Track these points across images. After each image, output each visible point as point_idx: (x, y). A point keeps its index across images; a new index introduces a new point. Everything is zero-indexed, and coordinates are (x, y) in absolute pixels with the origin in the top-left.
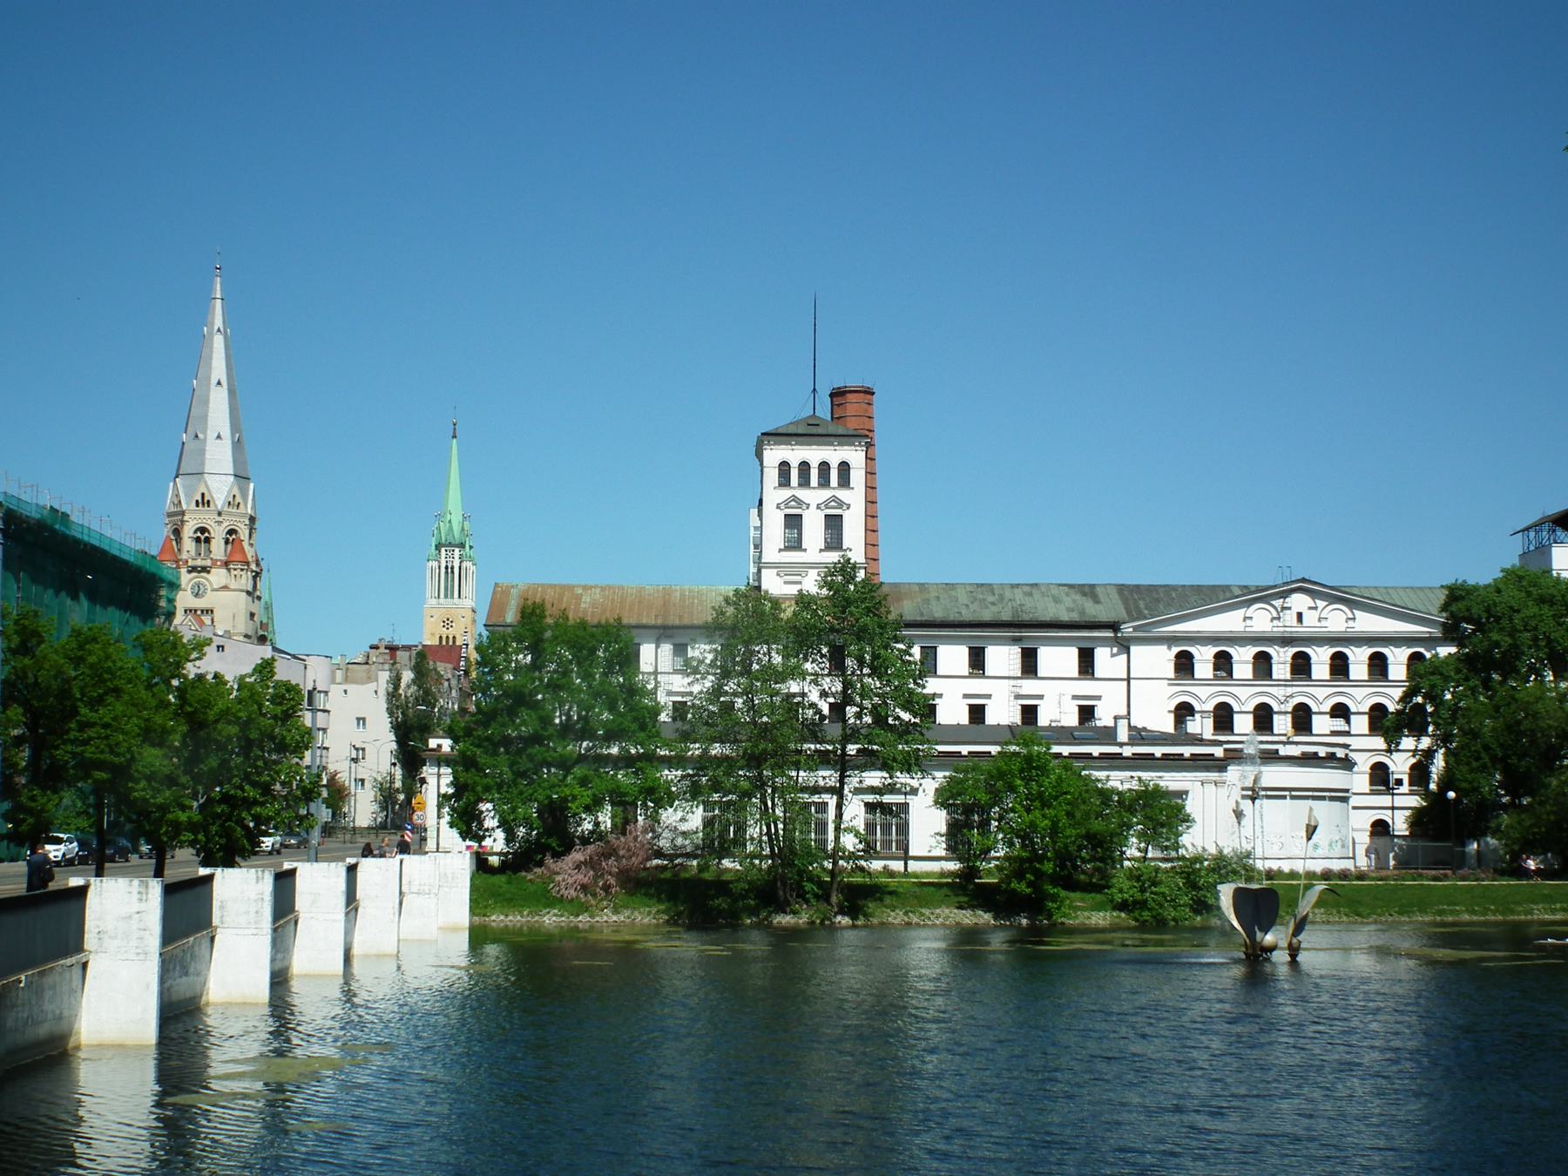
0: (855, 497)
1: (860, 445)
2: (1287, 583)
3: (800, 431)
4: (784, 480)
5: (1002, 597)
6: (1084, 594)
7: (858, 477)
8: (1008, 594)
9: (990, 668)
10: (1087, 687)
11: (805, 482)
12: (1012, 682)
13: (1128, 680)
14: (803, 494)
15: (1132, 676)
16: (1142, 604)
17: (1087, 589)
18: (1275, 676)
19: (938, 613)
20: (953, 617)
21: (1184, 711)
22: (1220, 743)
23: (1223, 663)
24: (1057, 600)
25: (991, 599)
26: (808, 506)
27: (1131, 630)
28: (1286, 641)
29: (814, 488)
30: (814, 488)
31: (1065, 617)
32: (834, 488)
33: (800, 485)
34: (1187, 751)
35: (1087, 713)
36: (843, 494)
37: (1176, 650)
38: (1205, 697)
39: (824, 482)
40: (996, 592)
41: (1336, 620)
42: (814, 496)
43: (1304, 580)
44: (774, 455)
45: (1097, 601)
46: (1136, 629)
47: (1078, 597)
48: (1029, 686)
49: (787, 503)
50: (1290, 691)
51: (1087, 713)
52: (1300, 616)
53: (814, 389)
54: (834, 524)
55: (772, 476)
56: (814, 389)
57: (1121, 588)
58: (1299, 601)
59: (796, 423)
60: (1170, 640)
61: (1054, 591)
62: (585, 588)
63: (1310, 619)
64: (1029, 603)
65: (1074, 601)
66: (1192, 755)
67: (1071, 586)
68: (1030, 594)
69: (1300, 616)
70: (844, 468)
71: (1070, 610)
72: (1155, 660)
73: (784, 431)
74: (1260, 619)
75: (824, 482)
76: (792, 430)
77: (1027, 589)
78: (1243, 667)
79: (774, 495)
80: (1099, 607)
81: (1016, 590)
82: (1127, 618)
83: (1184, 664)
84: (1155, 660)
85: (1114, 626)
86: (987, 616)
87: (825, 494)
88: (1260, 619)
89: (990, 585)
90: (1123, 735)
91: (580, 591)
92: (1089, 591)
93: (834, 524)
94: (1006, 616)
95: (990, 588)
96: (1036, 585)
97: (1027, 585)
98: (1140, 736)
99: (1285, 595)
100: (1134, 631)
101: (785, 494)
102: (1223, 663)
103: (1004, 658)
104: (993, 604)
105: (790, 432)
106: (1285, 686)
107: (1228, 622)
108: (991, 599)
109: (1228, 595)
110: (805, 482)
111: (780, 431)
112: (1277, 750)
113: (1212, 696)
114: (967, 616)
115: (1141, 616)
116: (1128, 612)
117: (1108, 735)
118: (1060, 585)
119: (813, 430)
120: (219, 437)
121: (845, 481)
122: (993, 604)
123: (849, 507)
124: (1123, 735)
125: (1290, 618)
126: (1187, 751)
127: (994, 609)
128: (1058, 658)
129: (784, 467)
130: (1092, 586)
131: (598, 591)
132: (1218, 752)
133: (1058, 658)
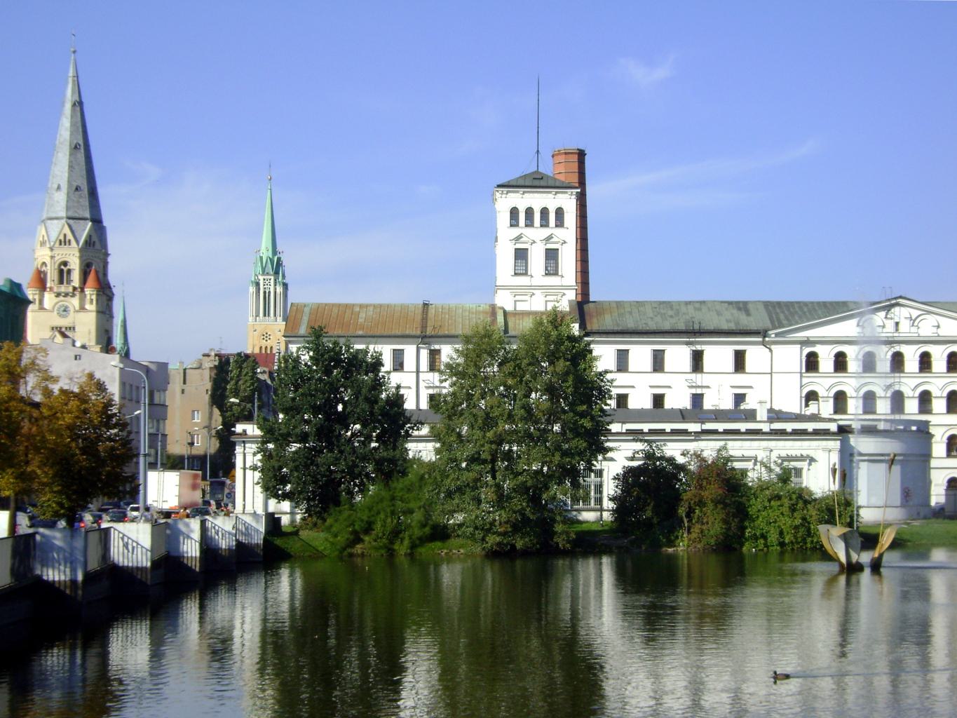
0: (569, 233)
1: (572, 194)
2: (889, 300)
3: (527, 184)
5: (677, 313)
6: (739, 309)
8: (683, 309)
9: (668, 366)
10: (740, 379)
11: (529, 222)
13: (771, 373)
14: (529, 232)
15: (773, 371)
16: (782, 316)
17: (741, 305)
19: (630, 324)
20: (641, 327)
21: (812, 396)
22: (835, 420)
24: (719, 314)
25: (670, 313)
26: (534, 242)
27: (773, 336)
28: (890, 342)
31: (725, 326)
33: (526, 226)
34: (810, 426)
35: (739, 398)
36: (560, 233)
37: (807, 350)
39: (545, 223)
40: (674, 307)
41: (927, 327)
42: (537, 233)
44: (506, 202)
45: (748, 313)
46: (777, 335)
47: (735, 311)
48: (698, 378)
49: (518, 239)
50: (890, 381)
51: (739, 398)
52: (897, 324)
55: (504, 218)
57: (768, 305)
61: (718, 307)
62: (361, 306)
63: (905, 327)
64: (698, 316)
65: (732, 314)
67: (730, 303)
68: (700, 309)
70: (560, 213)
71: (728, 321)
72: (789, 357)
73: (515, 184)
75: (545, 223)
76: (521, 182)
77: (697, 305)
79: (505, 233)
80: (751, 319)
81: (690, 307)
82: (771, 327)
83: (812, 363)
84: (789, 357)
86: (667, 326)
87: (545, 232)
89: (669, 302)
90: (762, 414)
91: (357, 309)
92: (743, 307)
93: (552, 255)
94: (682, 327)
95: (668, 304)
96: (704, 302)
97: (697, 302)
98: (775, 415)
99: (889, 308)
101: (515, 232)
102: (840, 363)
103: (679, 356)
104: (671, 317)
105: (518, 184)
106: (886, 377)
107: (847, 328)
108: (670, 313)
109: (845, 309)
110: (529, 222)
111: (511, 184)
112: (876, 425)
114: (652, 326)
115: (781, 326)
116: (772, 322)
117: (751, 415)
118: (722, 302)
119: (537, 183)
121: (560, 222)
122: (671, 317)
124: (762, 414)
125: (890, 326)
126: (810, 426)
127: (673, 321)
129: (514, 213)
130: (745, 303)
131: (371, 309)
132: (833, 427)
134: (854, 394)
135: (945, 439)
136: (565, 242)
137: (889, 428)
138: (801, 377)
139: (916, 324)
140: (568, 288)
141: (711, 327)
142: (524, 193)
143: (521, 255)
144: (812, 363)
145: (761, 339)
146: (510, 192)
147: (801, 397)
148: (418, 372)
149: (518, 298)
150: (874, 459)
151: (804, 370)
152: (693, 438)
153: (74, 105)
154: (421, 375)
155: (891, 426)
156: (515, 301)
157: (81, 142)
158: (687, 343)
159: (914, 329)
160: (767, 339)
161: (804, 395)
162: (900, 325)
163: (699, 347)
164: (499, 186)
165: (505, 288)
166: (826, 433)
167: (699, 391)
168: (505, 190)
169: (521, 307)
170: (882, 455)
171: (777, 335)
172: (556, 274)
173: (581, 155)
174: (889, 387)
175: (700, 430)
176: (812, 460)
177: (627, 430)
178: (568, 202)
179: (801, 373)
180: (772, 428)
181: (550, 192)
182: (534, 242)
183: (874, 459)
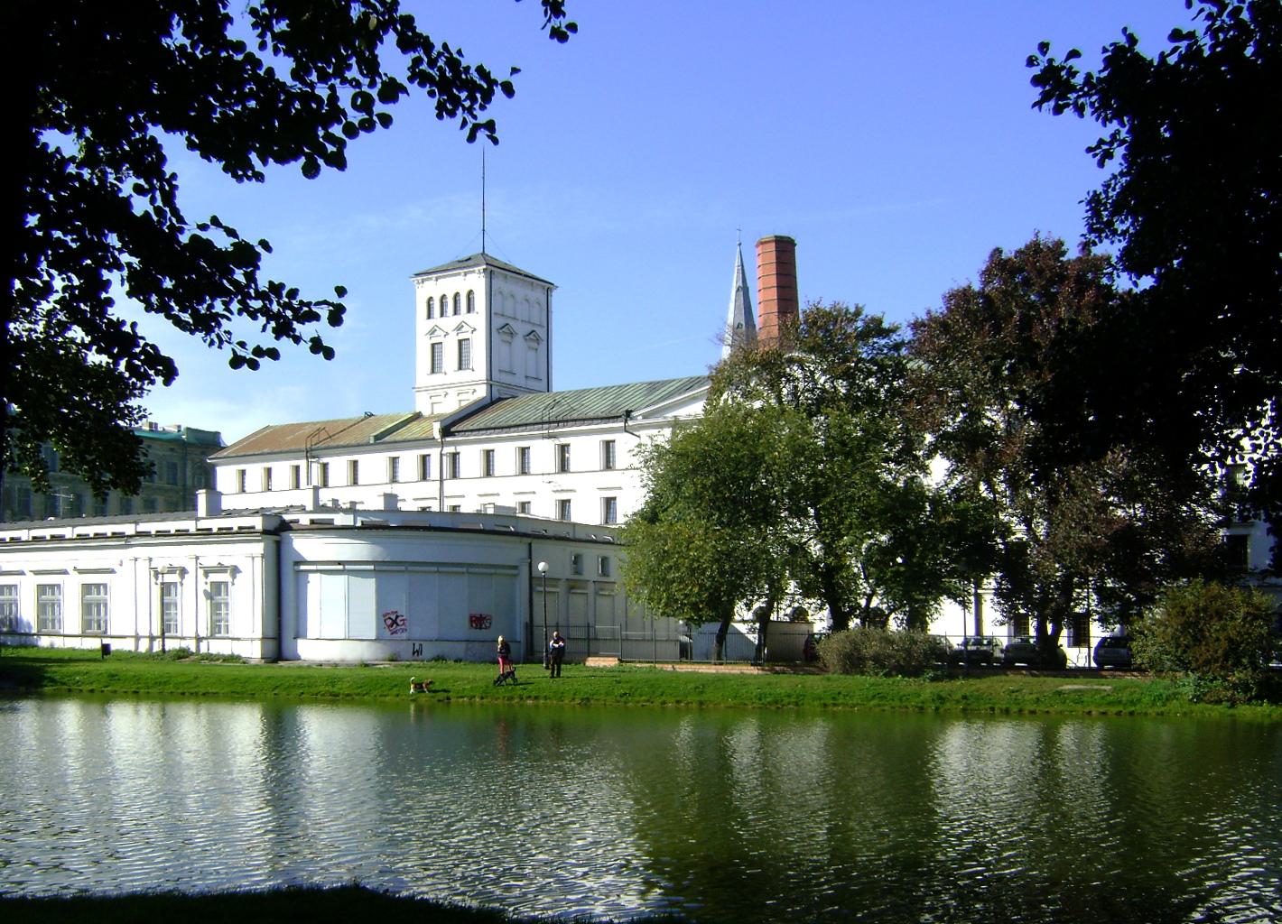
0: (478, 319)
26: (447, 334)
27: (640, 417)
42: (450, 322)
46: (645, 417)
48: (564, 480)
79: (423, 325)
87: (457, 320)
101: (431, 323)
136: (475, 330)
137: (352, 524)
142: (437, 279)
145: (622, 424)
146: (440, 277)
149: (434, 400)
150: (343, 567)
152: (123, 543)
153: (738, 290)
155: (355, 521)
156: (433, 404)
157: (743, 323)
158: (550, 437)
163: (563, 441)
164: (417, 275)
166: (245, 531)
167: (564, 496)
168: (420, 278)
170: (339, 563)
171: (645, 417)
175: (133, 533)
176: (235, 571)
177: (78, 535)
180: (199, 527)
181: (459, 274)
182: (447, 334)
183: (343, 567)
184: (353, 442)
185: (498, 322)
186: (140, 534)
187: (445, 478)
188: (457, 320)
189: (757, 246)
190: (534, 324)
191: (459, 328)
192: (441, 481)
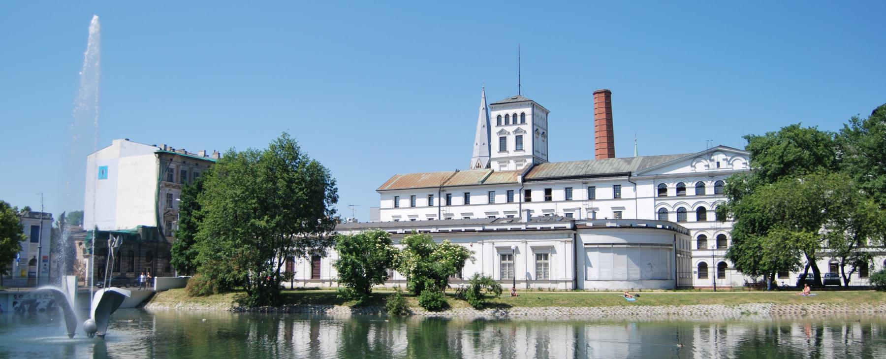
0: (528, 128)
4: (499, 123)
7: (528, 119)
10: (618, 203)
12: (584, 203)
14: (507, 128)
18: (706, 193)
20: (561, 175)
21: (663, 212)
23: (681, 189)
26: (509, 133)
28: (711, 176)
29: (511, 125)
30: (511, 125)
32: (519, 124)
36: (523, 127)
38: (671, 204)
42: (511, 129)
43: (720, 146)
48: (594, 204)
49: (501, 132)
52: (718, 163)
53: (519, 85)
54: (519, 140)
56: (519, 85)
58: (719, 157)
59: (507, 99)
60: (654, 179)
66: (541, 228)
69: (718, 163)
70: (523, 115)
72: (648, 190)
74: (701, 167)
75: (515, 122)
78: (691, 191)
79: (495, 130)
83: (662, 190)
84: (648, 190)
85: (629, 174)
87: (515, 127)
88: (701, 167)
93: (519, 140)
100: (638, 175)
101: (500, 129)
102: (681, 189)
103: (580, 193)
107: (687, 170)
110: (507, 123)
113: (675, 206)
114: (566, 174)
120: (484, 144)
121: (523, 121)
123: (525, 132)
125: (713, 165)
128: (604, 192)
129: (499, 117)
133: (604, 192)
134: (690, 209)
135: (715, 237)
138: (655, 200)
139: (731, 163)
140: (528, 157)
141: (599, 173)
143: (503, 141)
144: (662, 190)
147: (655, 212)
148: (440, 206)
151: (657, 195)
154: (441, 208)
159: (731, 166)
160: (631, 178)
161: (657, 211)
162: (721, 164)
165: (495, 159)
169: (503, 169)
172: (521, 150)
173: (608, 94)
174: (714, 203)
178: (528, 111)
179: (654, 197)
183: (602, 248)
184: (464, 184)
185: (535, 128)
186: (484, 231)
187: (522, 201)
188: (515, 127)
189: (594, 94)
190: (539, 127)
191: (516, 131)
192: (520, 203)
